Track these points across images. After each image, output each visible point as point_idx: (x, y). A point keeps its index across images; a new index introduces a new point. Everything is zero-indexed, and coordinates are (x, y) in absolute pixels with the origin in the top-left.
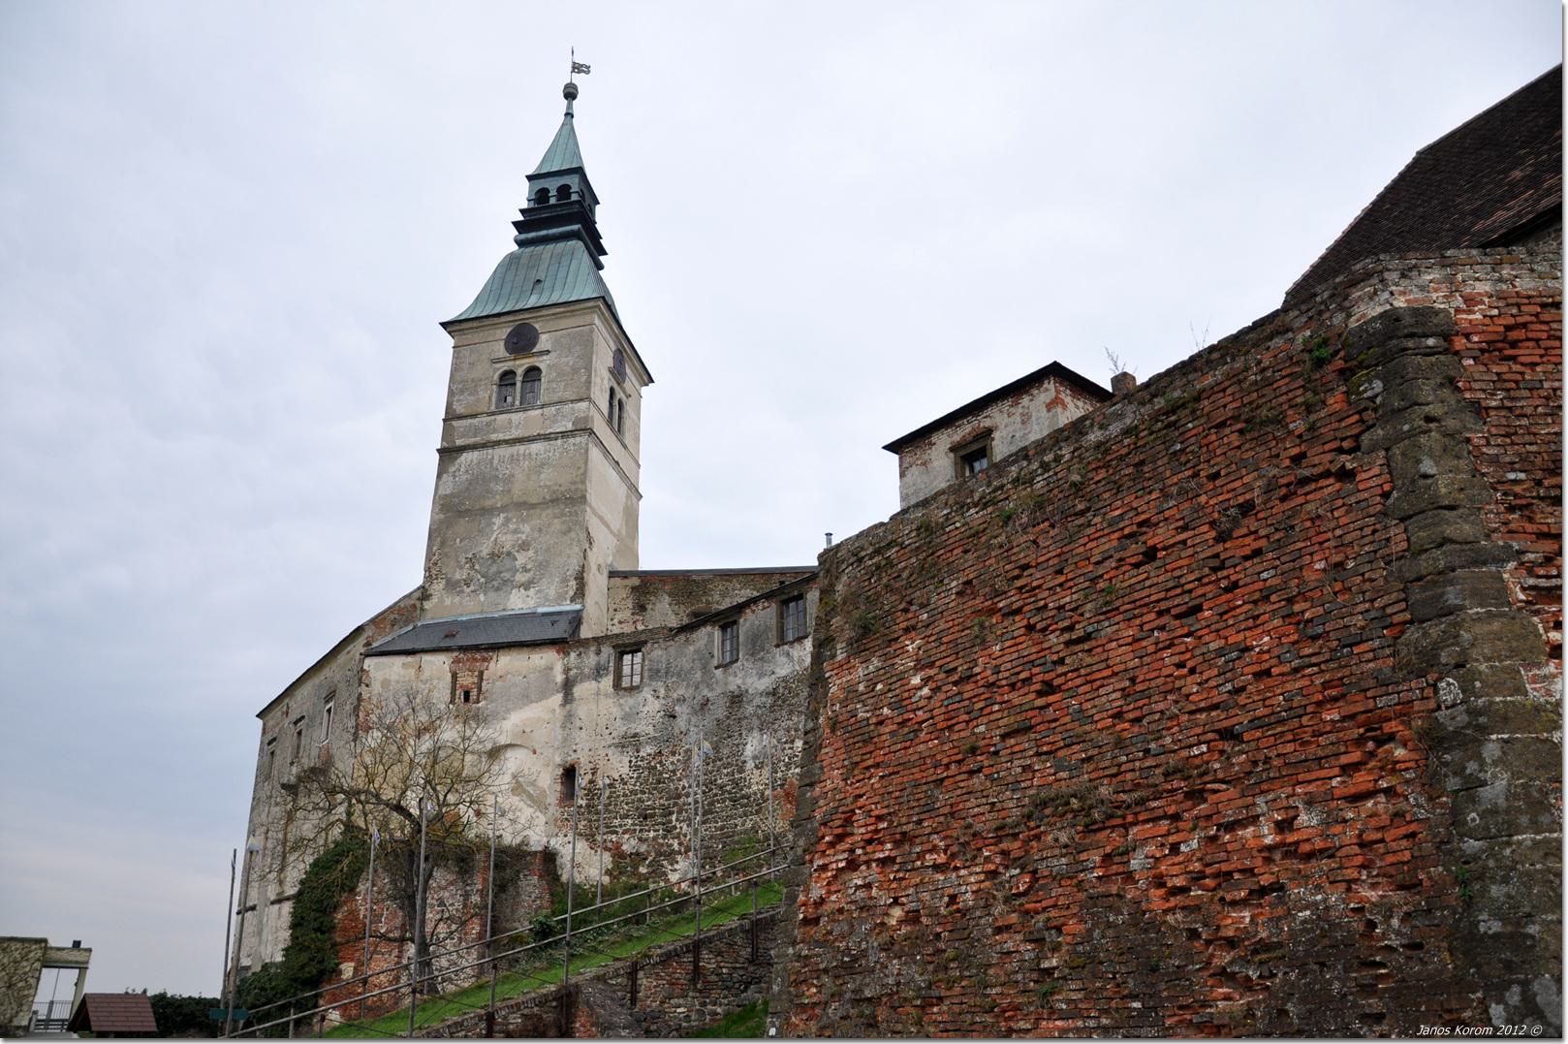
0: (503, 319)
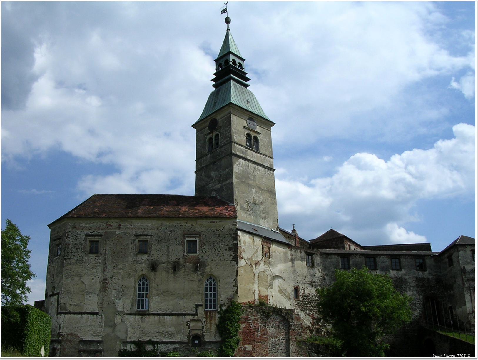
0: (248, 113)
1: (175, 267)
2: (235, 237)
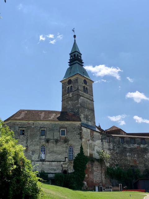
1: (57, 141)
2: (81, 130)
